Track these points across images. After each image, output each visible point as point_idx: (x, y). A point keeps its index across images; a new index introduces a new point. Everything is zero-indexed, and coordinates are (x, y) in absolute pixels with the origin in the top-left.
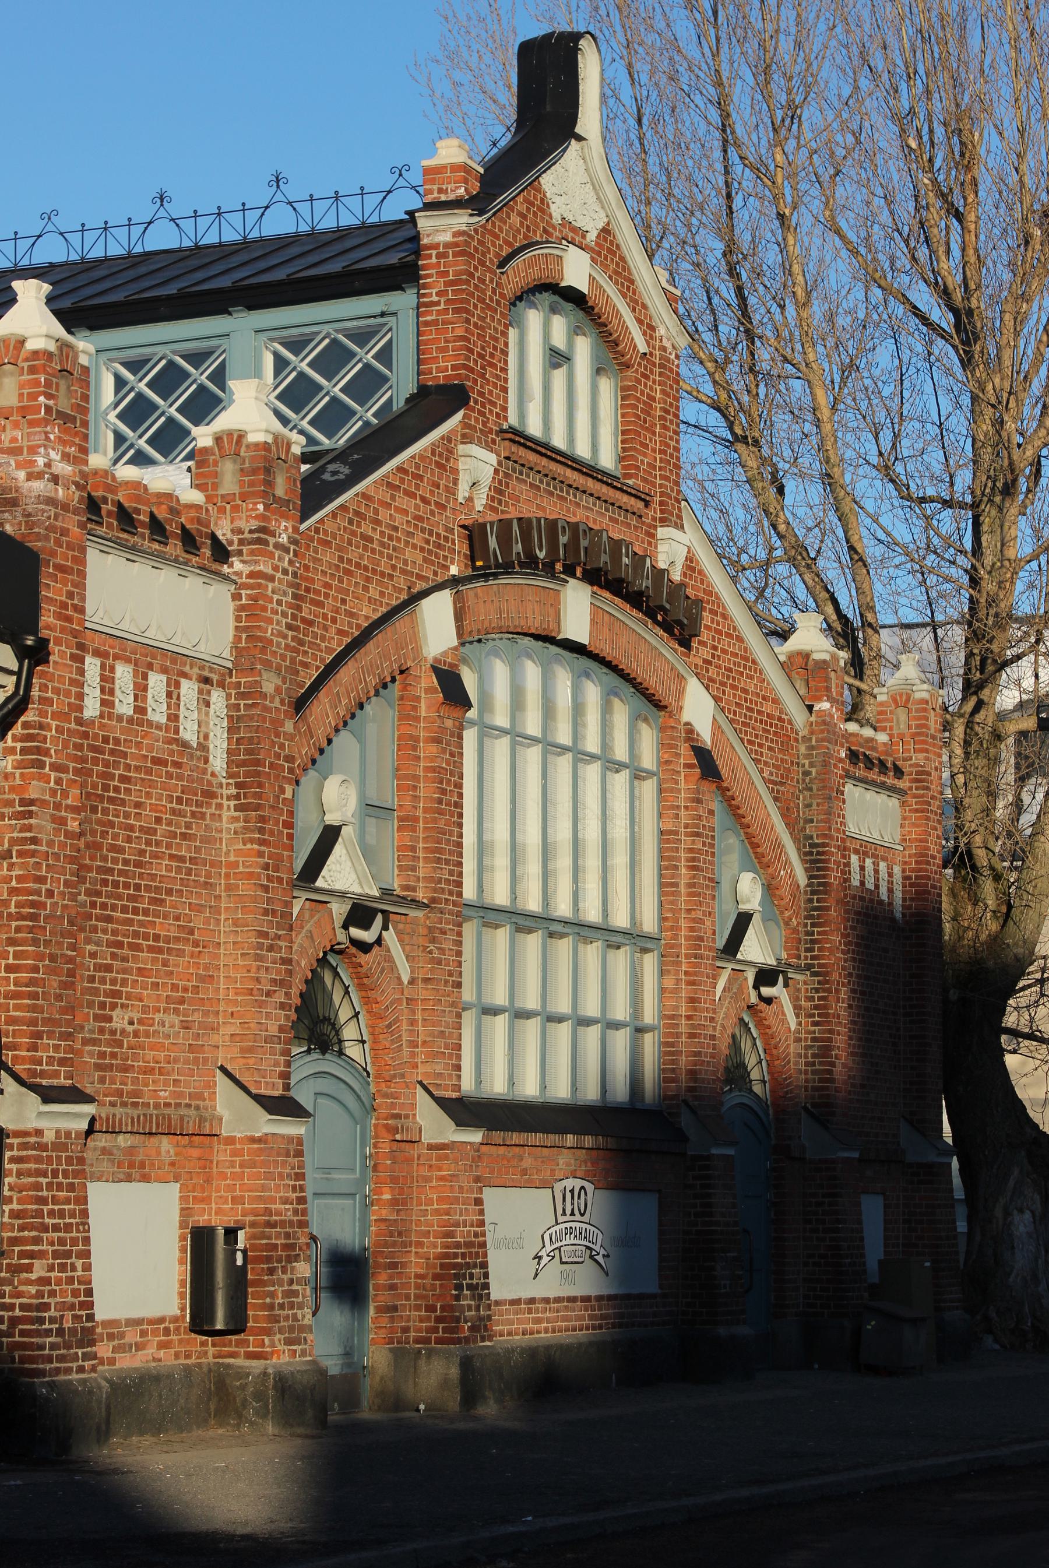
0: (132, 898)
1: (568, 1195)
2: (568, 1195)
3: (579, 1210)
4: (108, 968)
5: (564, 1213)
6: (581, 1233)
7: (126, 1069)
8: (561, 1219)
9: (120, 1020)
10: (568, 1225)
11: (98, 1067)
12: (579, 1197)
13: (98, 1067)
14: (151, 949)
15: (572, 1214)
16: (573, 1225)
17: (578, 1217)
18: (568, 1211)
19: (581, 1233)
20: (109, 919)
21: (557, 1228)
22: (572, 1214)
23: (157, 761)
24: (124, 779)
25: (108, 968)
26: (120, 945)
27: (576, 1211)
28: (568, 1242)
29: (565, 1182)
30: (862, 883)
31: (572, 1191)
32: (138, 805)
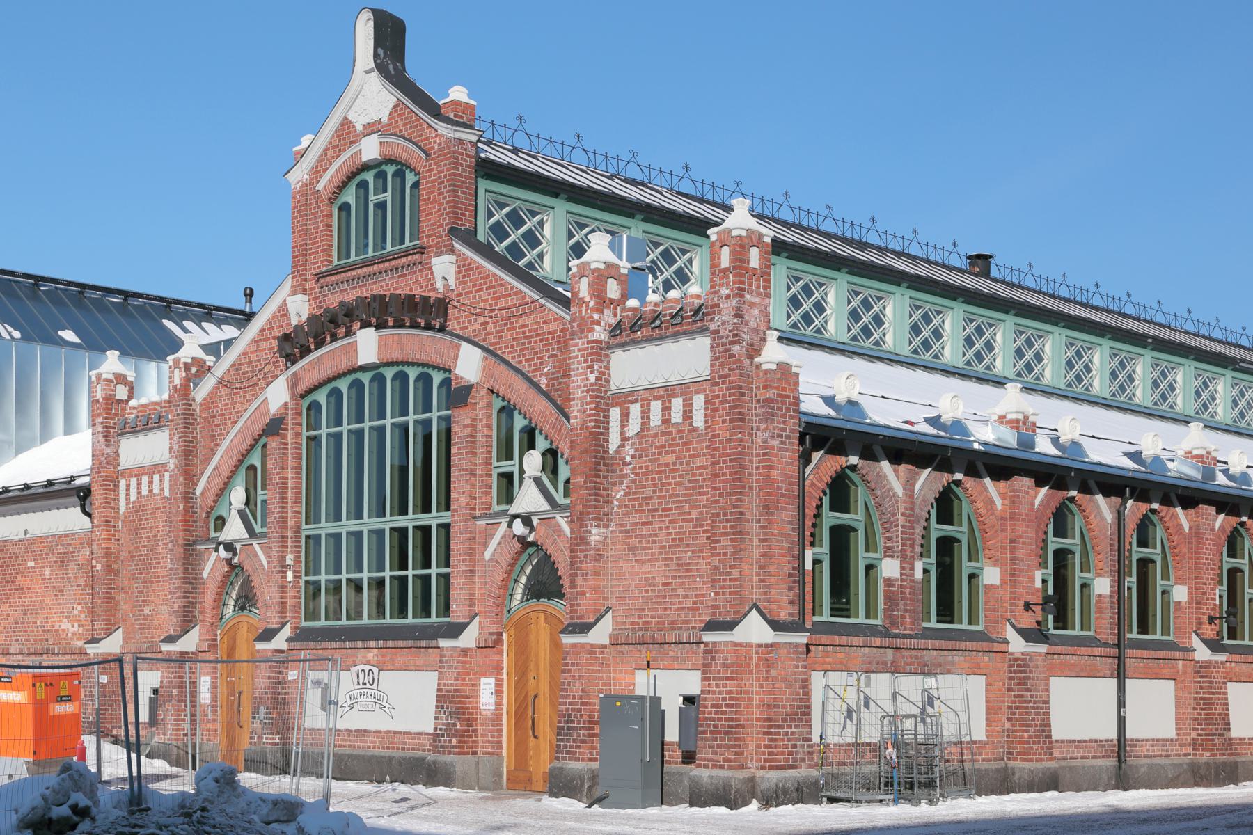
0: (150, 564)
4: (142, 592)
7: (148, 629)
9: (146, 611)
11: (140, 629)
13: (140, 629)
14: (157, 582)
17: (368, 686)
20: (142, 573)
22: (364, 684)
23: (157, 508)
24: (147, 519)
25: (142, 592)
26: (146, 582)
30: (666, 421)
32: (151, 528)
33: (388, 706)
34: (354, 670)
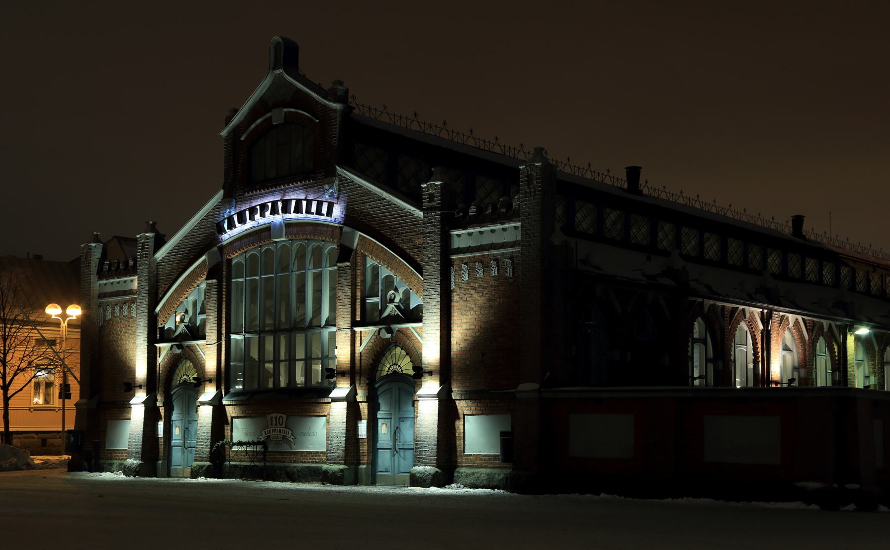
1: (274, 420)
2: (274, 420)
3: (279, 424)
5: (272, 424)
6: (280, 431)
8: (269, 426)
10: (274, 428)
12: (279, 419)
15: (276, 424)
16: (277, 428)
17: (279, 426)
18: (274, 423)
19: (280, 431)
21: (268, 429)
22: (276, 424)
27: (278, 424)
28: (274, 434)
29: (272, 415)
31: (276, 418)
33: (292, 437)
34: (269, 417)
